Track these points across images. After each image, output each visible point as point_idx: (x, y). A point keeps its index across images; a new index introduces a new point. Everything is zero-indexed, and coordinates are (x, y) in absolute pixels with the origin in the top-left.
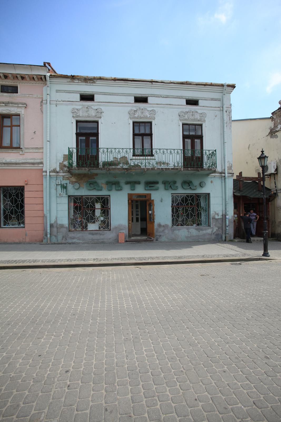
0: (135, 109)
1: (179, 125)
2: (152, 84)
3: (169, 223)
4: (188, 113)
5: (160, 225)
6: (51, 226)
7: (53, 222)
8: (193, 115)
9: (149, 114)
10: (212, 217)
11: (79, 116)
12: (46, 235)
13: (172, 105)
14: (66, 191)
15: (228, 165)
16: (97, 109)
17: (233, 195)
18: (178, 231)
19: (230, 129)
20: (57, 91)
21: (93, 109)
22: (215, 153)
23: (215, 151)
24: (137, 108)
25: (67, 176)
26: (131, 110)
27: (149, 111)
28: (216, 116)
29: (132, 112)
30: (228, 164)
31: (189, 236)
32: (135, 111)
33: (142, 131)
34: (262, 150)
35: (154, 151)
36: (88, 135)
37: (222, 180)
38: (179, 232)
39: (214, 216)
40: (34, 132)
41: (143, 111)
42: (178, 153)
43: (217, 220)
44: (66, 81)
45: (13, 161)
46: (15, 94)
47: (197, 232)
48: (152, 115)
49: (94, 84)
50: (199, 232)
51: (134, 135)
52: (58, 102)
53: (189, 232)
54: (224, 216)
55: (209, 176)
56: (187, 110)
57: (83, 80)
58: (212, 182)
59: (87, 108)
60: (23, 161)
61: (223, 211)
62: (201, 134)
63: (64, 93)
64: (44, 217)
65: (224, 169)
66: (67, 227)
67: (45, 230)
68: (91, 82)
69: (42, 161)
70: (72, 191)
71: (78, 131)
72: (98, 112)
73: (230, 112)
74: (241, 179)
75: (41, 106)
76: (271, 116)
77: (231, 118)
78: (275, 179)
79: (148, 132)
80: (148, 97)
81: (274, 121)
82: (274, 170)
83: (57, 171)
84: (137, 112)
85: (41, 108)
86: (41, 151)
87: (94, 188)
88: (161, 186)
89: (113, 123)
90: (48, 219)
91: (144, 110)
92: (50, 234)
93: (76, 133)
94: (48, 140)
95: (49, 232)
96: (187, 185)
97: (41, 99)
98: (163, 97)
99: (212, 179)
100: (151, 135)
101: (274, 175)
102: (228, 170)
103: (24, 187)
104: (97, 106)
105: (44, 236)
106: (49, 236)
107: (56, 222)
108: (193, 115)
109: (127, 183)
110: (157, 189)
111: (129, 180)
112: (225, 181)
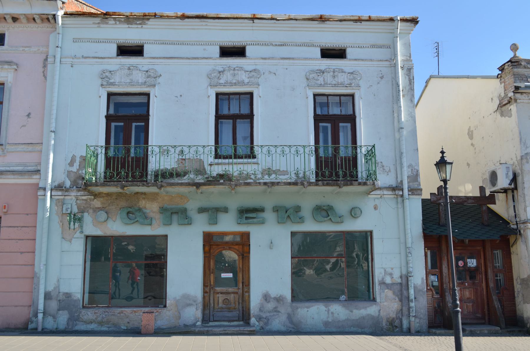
0: (221, 69)
1: (307, 98)
2: (253, 22)
3: (288, 294)
4: (325, 74)
5: (266, 297)
6: (48, 296)
7: (50, 288)
8: (334, 77)
10: (379, 281)
11: (113, 84)
12: (36, 316)
13: (293, 59)
14: (81, 227)
15: (410, 173)
16: (147, 71)
17: (422, 234)
18: (306, 309)
19: (412, 101)
20: (75, 40)
21: (140, 70)
22: (373, 151)
23: (374, 146)
24: (225, 66)
25: (84, 198)
26: (214, 70)
27: (249, 73)
28: (382, 78)
29: (215, 74)
30: (410, 170)
31: (330, 320)
32: (220, 72)
33: (234, 110)
34: (442, 149)
35: (256, 149)
36: (128, 119)
37: (397, 202)
38: (308, 311)
39: (383, 279)
40: (27, 114)
41: (236, 72)
42: (297, 153)
43: (388, 286)
44: (91, 22)
47: (347, 312)
48: (252, 79)
49: (144, 26)
50: (352, 312)
51: (218, 117)
52: (76, 60)
53: (328, 311)
54: (406, 278)
55: (369, 196)
56: (323, 68)
57: (123, 20)
58: (376, 208)
59: (129, 69)
61: (403, 268)
62: (351, 113)
63: (88, 43)
64: (33, 278)
65: (402, 181)
66: (78, 298)
67: (33, 304)
68: (138, 22)
69: (39, 168)
71: (112, 112)
72: (149, 77)
73: (411, 69)
74: (440, 200)
75: (45, 66)
76: (499, 74)
77: (412, 81)
78: (514, 201)
79: (245, 111)
80: (246, 46)
81: (503, 84)
82: (508, 182)
83: (65, 187)
84: (224, 75)
85: (44, 71)
86: (38, 148)
87: (136, 220)
88: (269, 216)
89: (177, 97)
90: (42, 281)
91: (238, 70)
92: (44, 313)
93: (106, 116)
94: (53, 129)
95: (42, 309)
96: (324, 213)
97: (45, 55)
98: (276, 45)
99: (377, 202)
100: (250, 117)
101: (513, 192)
102: (408, 183)
104: (149, 66)
105: (31, 315)
106: (40, 316)
107: (57, 287)
108: (334, 77)
109: (202, 210)
110: (263, 223)
111: (205, 204)
112: (404, 205)
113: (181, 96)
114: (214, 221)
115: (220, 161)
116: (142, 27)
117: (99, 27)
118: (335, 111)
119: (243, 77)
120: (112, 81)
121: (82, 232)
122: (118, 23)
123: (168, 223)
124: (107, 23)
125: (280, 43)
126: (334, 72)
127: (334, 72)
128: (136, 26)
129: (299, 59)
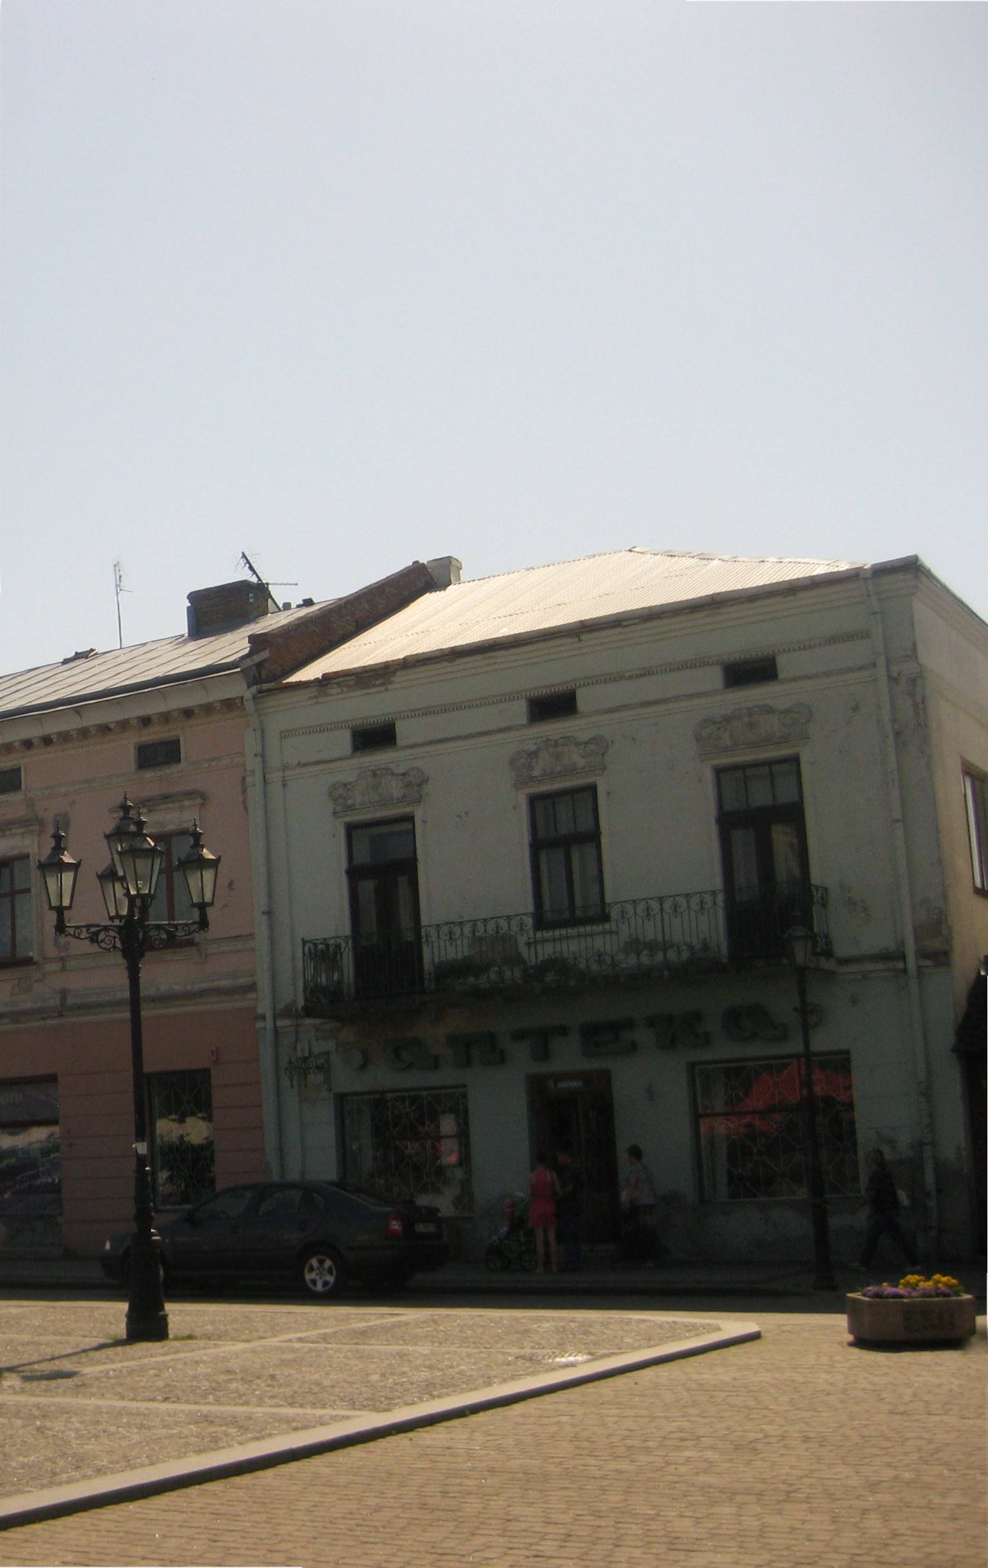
0: (532, 748)
2: (580, 640)
9: (583, 757)
14: (328, 1080)
20: (285, 735)
29: (522, 761)
45: (176, 987)
46: (174, 769)
49: (389, 687)
60: (203, 986)
68: (378, 682)
70: (346, 1080)
77: (921, 706)
79: (585, 825)
91: (562, 745)
100: (593, 837)
103: (206, 1072)
109: (519, 1036)
110: (633, 1048)
113: (467, 813)
114: (543, 1053)
115: (548, 934)
116: (386, 689)
117: (317, 703)
118: (760, 796)
119: (577, 758)
120: (350, 802)
121: (330, 1090)
122: (345, 689)
123: (467, 1063)
124: (329, 695)
125: (638, 672)
126: (750, 715)
127: (750, 715)
128: (376, 689)
129: (677, 698)
